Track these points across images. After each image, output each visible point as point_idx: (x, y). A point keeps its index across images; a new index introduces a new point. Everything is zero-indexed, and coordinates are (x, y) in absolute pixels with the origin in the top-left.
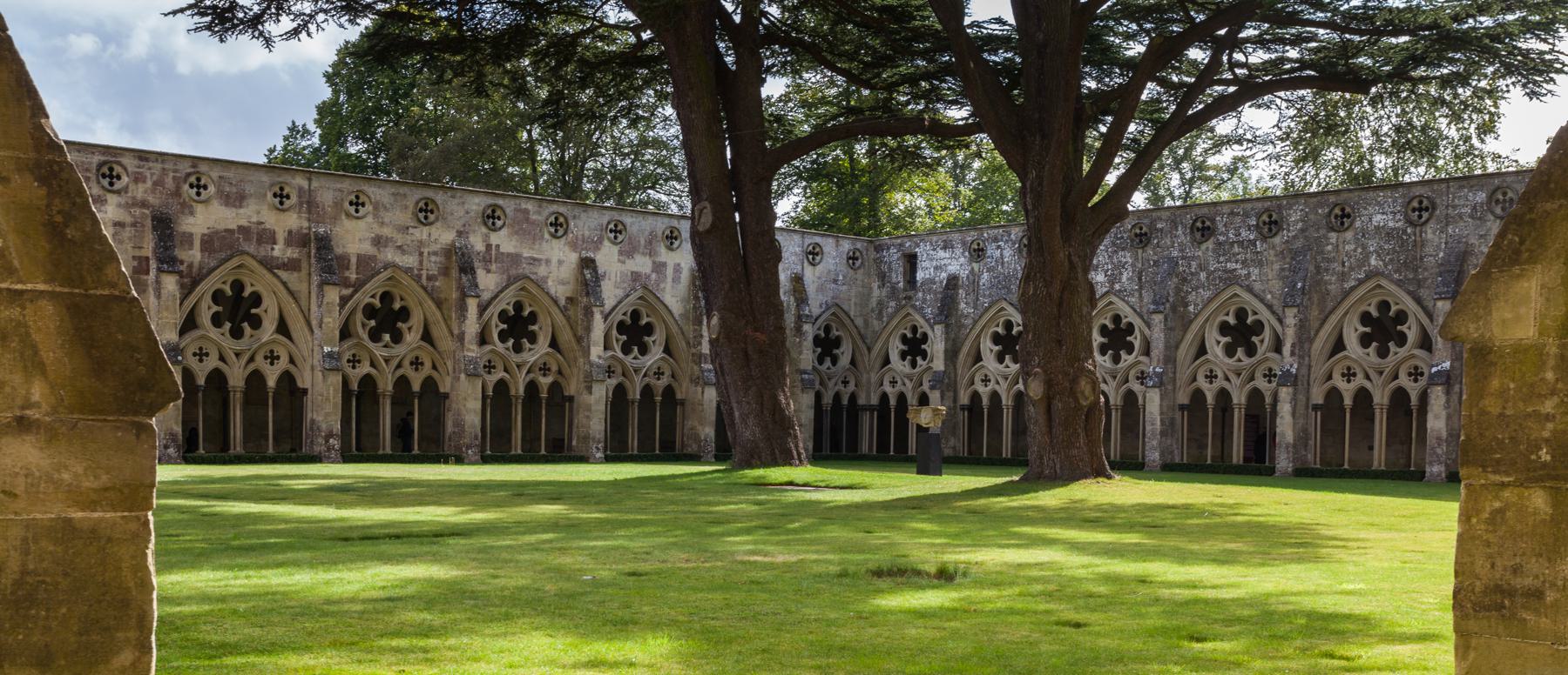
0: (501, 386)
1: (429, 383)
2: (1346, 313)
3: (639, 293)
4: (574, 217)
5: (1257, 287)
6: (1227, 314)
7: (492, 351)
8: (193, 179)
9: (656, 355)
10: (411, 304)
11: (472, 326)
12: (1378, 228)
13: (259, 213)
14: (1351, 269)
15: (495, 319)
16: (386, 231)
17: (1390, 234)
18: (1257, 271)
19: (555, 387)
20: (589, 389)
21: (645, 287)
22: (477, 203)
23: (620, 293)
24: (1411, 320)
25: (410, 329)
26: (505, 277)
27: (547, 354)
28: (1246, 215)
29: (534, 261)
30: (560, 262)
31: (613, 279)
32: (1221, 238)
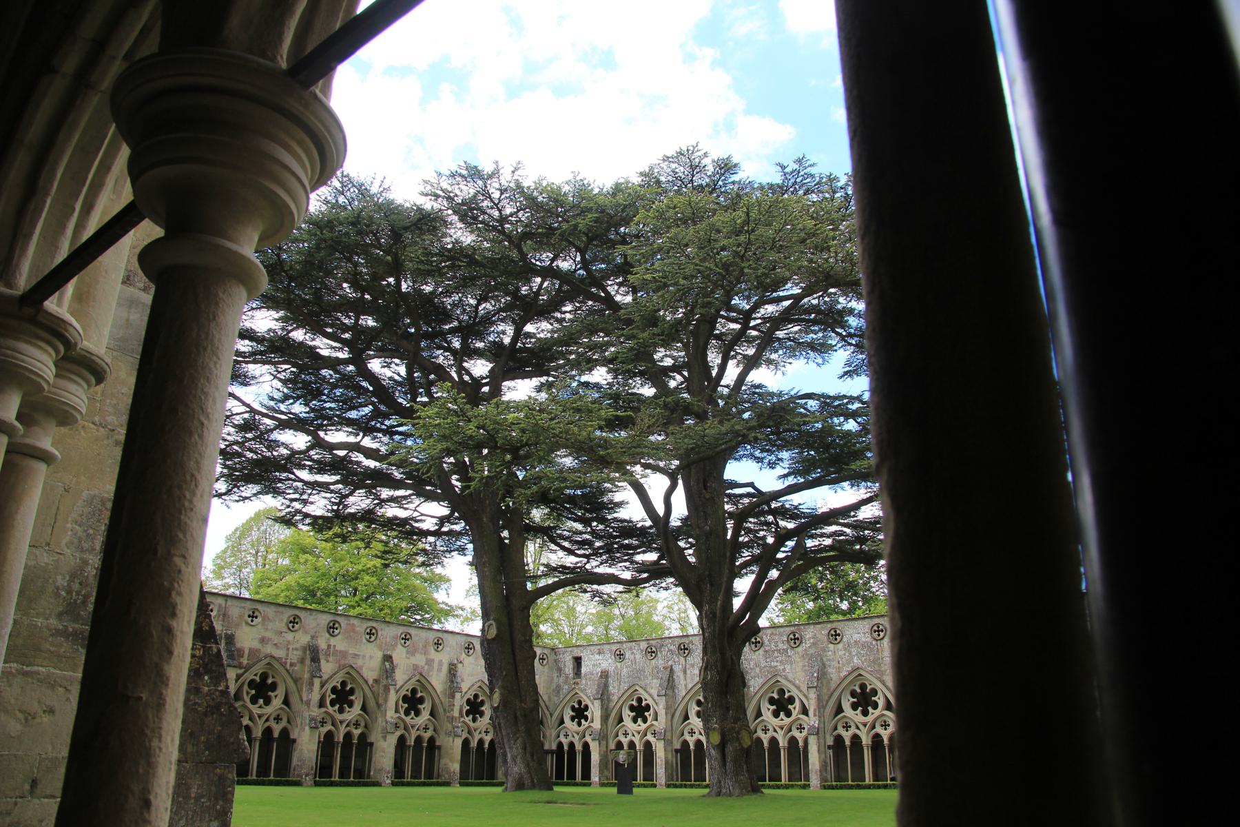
0: (329, 735)
1: (285, 733)
3: (417, 678)
4: (381, 630)
5: (790, 676)
6: (773, 692)
7: (326, 712)
9: (425, 716)
10: (278, 680)
11: (315, 697)
12: (855, 642)
15: (329, 691)
16: (268, 634)
17: (863, 646)
18: (789, 667)
19: (363, 737)
20: (385, 738)
21: (421, 674)
23: (406, 677)
24: (880, 693)
25: (276, 696)
26: (337, 665)
27: (359, 715)
28: (781, 635)
29: (356, 656)
30: (371, 657)
31: (402, 668)
32: (767, 648)
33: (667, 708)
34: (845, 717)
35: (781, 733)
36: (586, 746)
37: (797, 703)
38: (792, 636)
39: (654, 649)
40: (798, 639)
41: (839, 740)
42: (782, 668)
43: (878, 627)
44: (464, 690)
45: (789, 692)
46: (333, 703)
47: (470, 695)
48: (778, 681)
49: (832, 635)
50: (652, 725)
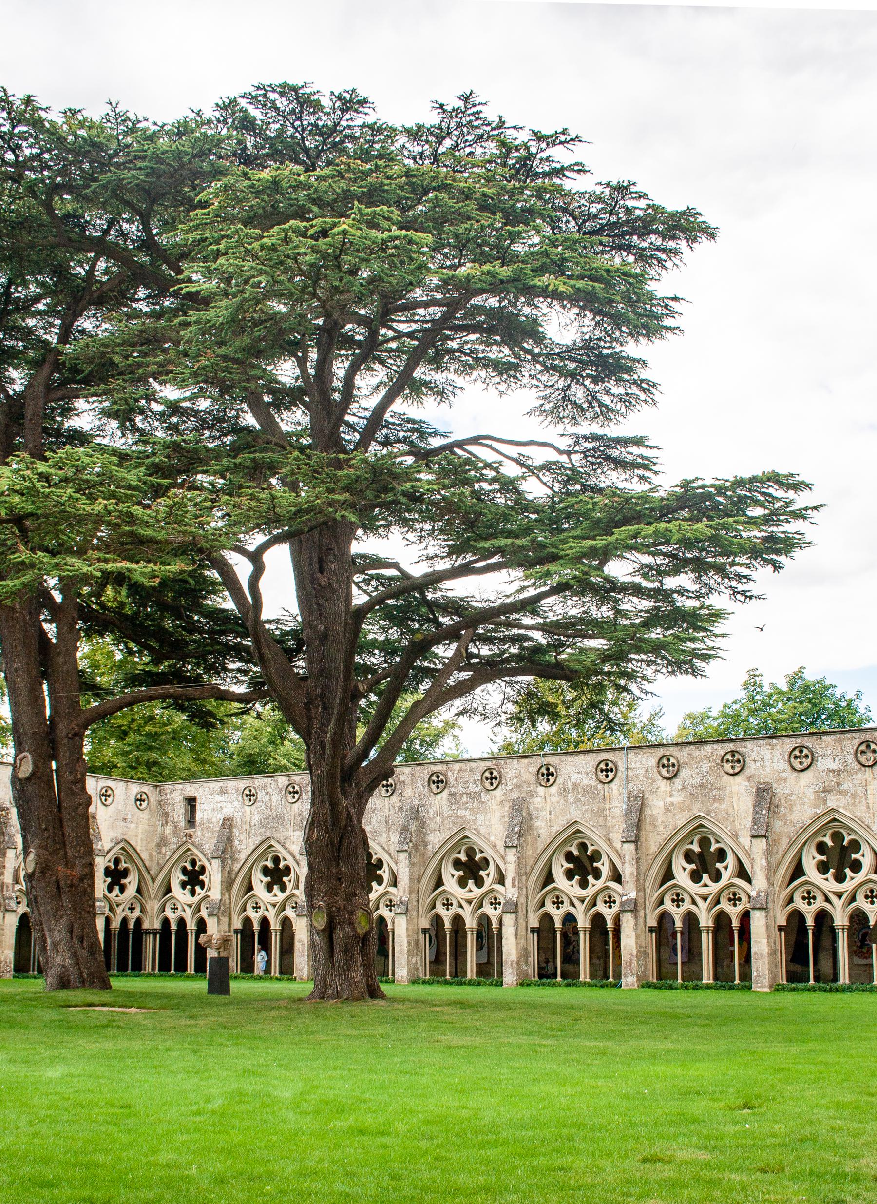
5: (483, 830)
12: (575, 784)
18: (482, 817)
24: (604, 858)
32: (453, 790)
35: (468, 909)
36: (286, 923)
38: (487, 774)
39: (297, 788)
43: (607, 765)
45: (482, 852)
49: (543, 775)
50: (293, 895)
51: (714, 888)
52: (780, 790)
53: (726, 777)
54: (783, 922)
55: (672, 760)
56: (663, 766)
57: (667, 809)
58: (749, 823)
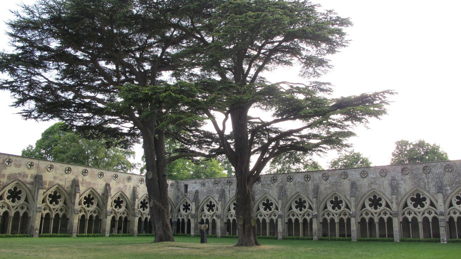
0: (83, 216)
2: (292, 201)
3: (120, 193)
4: (105, 173)
5: (271, 195)
7: (82, 207)
8: (8, 160)
9: (123, 208)
10: (61, 194)
12: (298, 182)
13: (24, 169)
14: (293, 191)
15: (83, 198)
16: (57, 175)
19: (97, 217)
20: (106, 218)
21: (122, 191)
22: (81, 168)
23: (116, 193)
24: (307, 203)
25: (60, 201)
26: (87, 188)
27: (96, 208)
28: (268, 178)
30: (101, 184)
32: (263, 183)
33: (222, 206)
34: (293, 211)
36: (189, 221)
37: (274, 205)
38: (273, 179)
40: (275, 180)
41: (290, 220)
42: (268, 191)
44: (139, 198)
45: (271, 201)
46: (85, 203)
47: (142, 200)
48: (266, 196)
50: (216, 213)
51: (339, 211)
52: (358, 183)
53: (342, 179)
54: (287, 222)
55: (326, 175)
56: (324, 176)
57: (325, 189)
58: (349, 192)
